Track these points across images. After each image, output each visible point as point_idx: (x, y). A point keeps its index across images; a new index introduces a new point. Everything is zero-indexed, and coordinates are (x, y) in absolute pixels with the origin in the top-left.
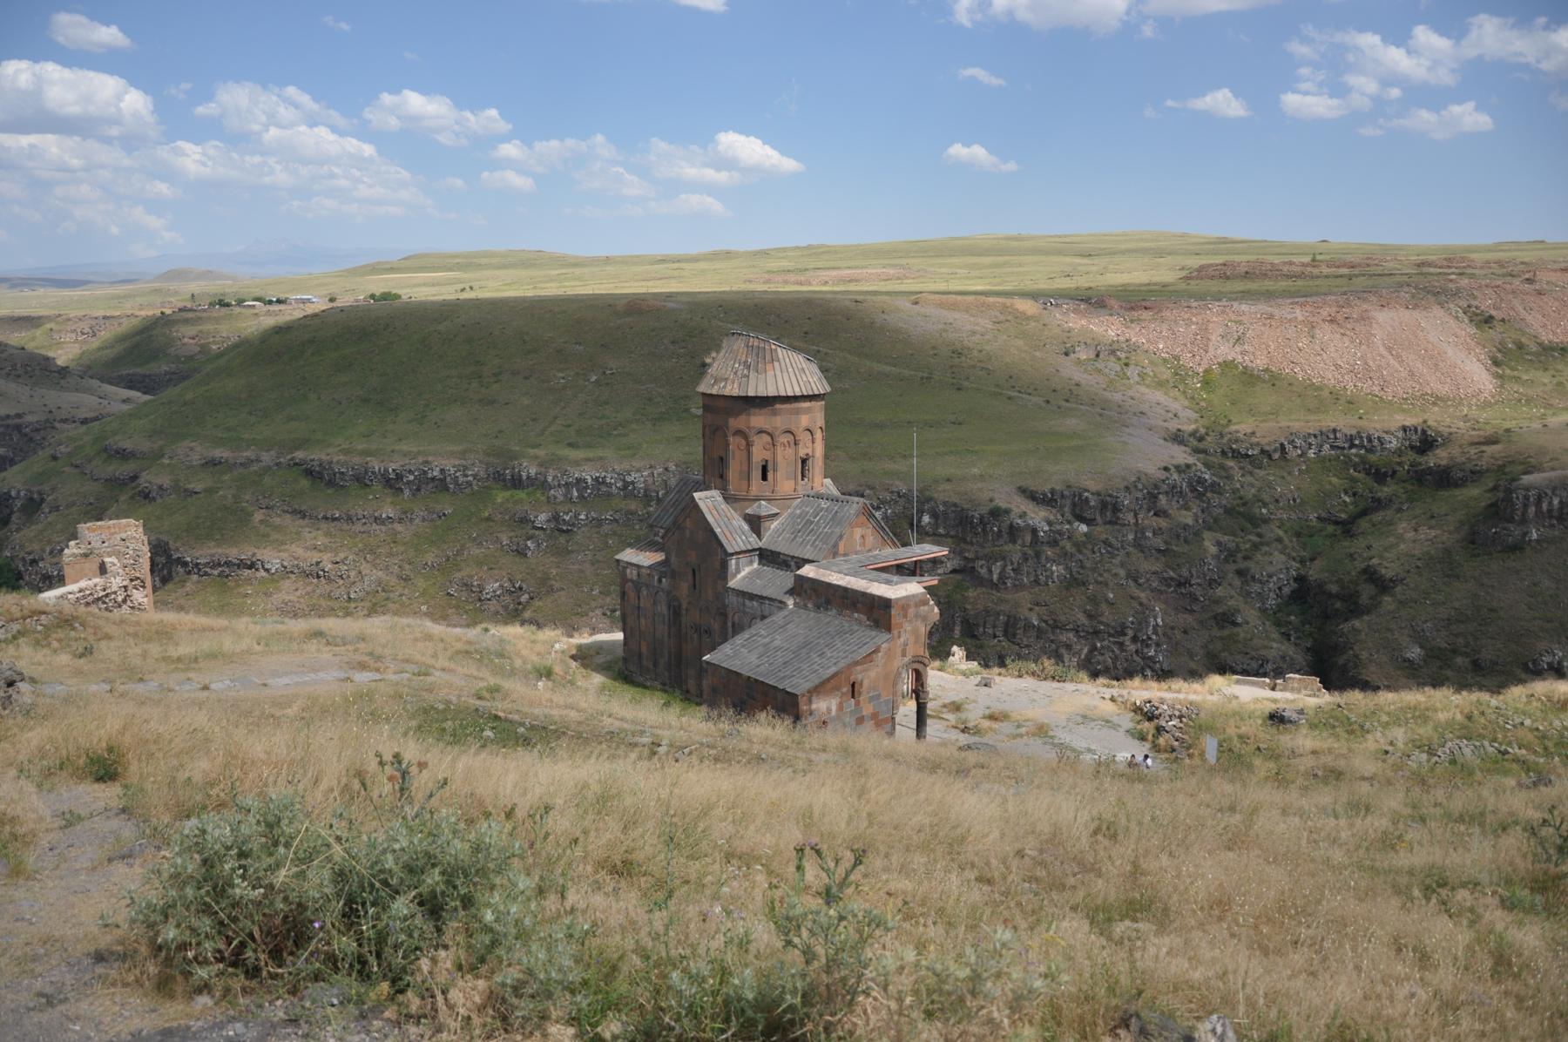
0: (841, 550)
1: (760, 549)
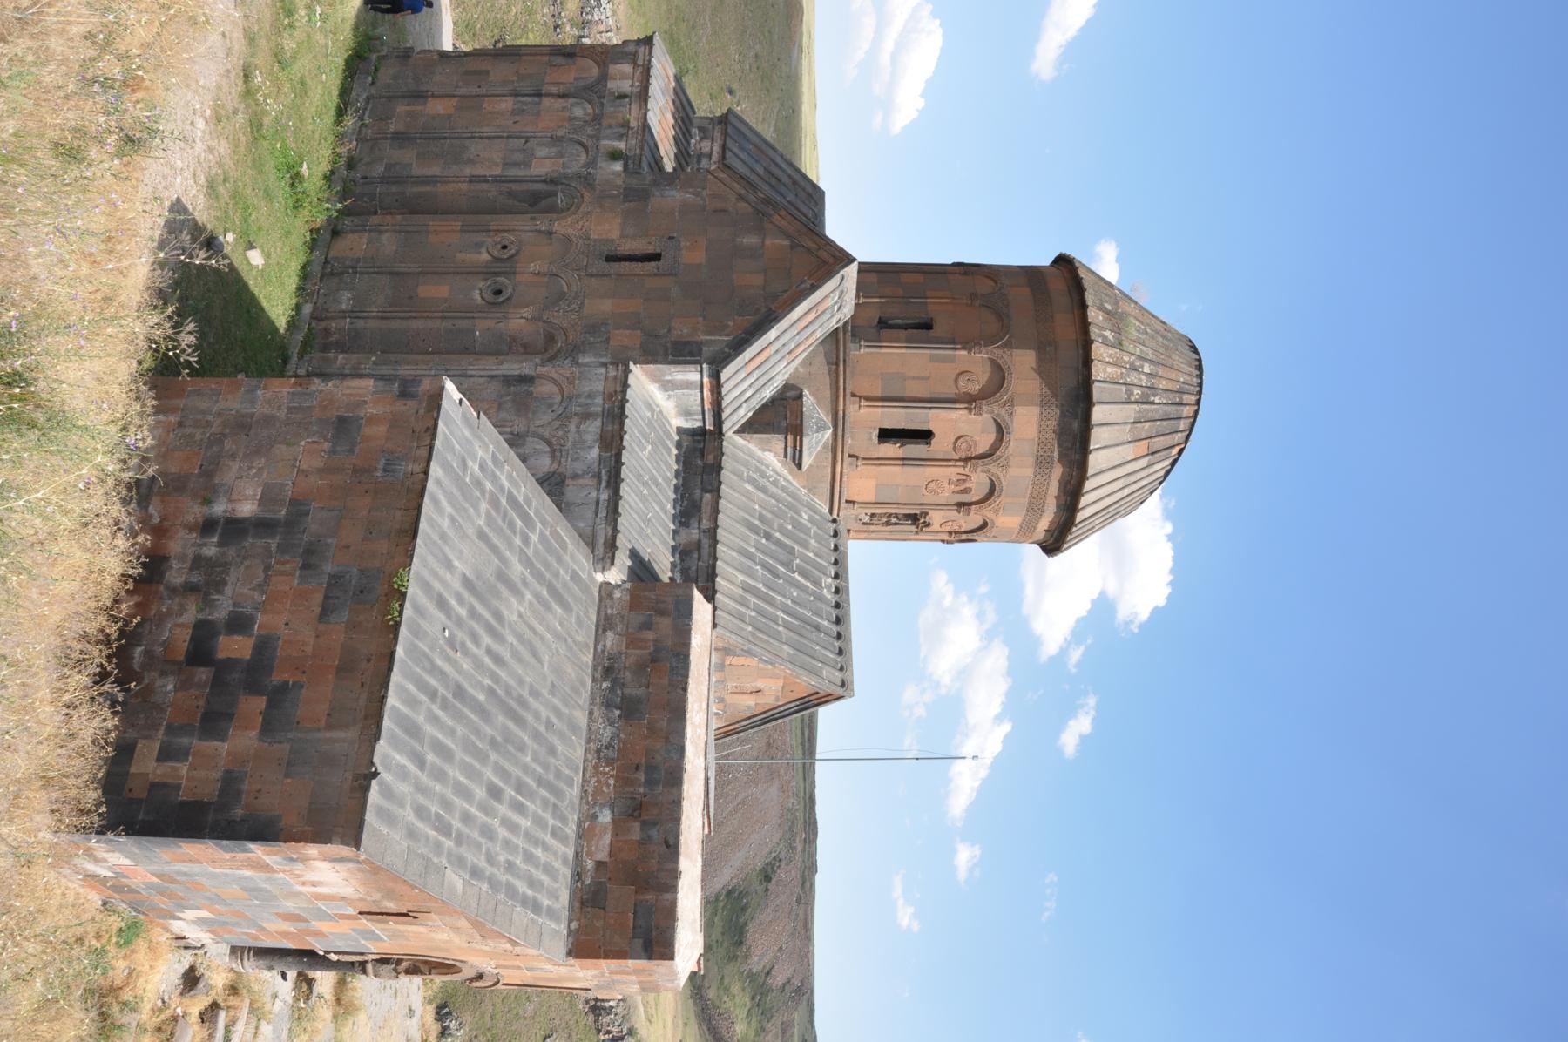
0: (728, 660)
1: (719, 432)
